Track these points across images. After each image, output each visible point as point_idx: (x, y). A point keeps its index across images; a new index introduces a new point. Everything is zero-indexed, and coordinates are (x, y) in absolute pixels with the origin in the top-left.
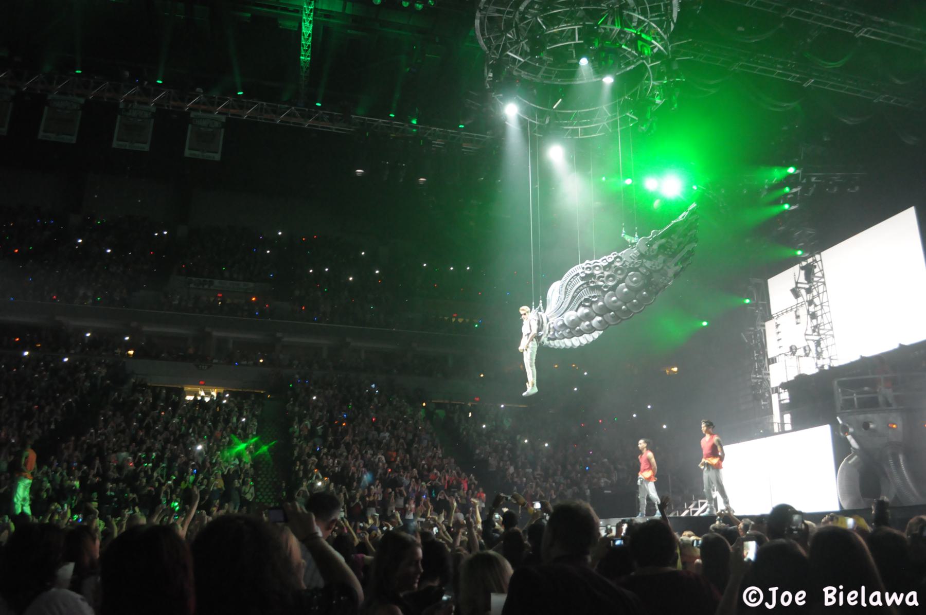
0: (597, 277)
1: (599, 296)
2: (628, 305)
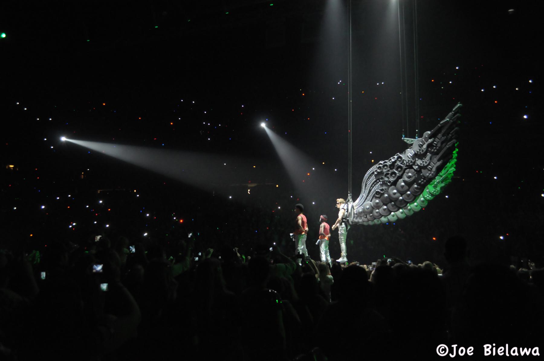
0: (384, 174)
1: (385, 189)
2: (403, 196)
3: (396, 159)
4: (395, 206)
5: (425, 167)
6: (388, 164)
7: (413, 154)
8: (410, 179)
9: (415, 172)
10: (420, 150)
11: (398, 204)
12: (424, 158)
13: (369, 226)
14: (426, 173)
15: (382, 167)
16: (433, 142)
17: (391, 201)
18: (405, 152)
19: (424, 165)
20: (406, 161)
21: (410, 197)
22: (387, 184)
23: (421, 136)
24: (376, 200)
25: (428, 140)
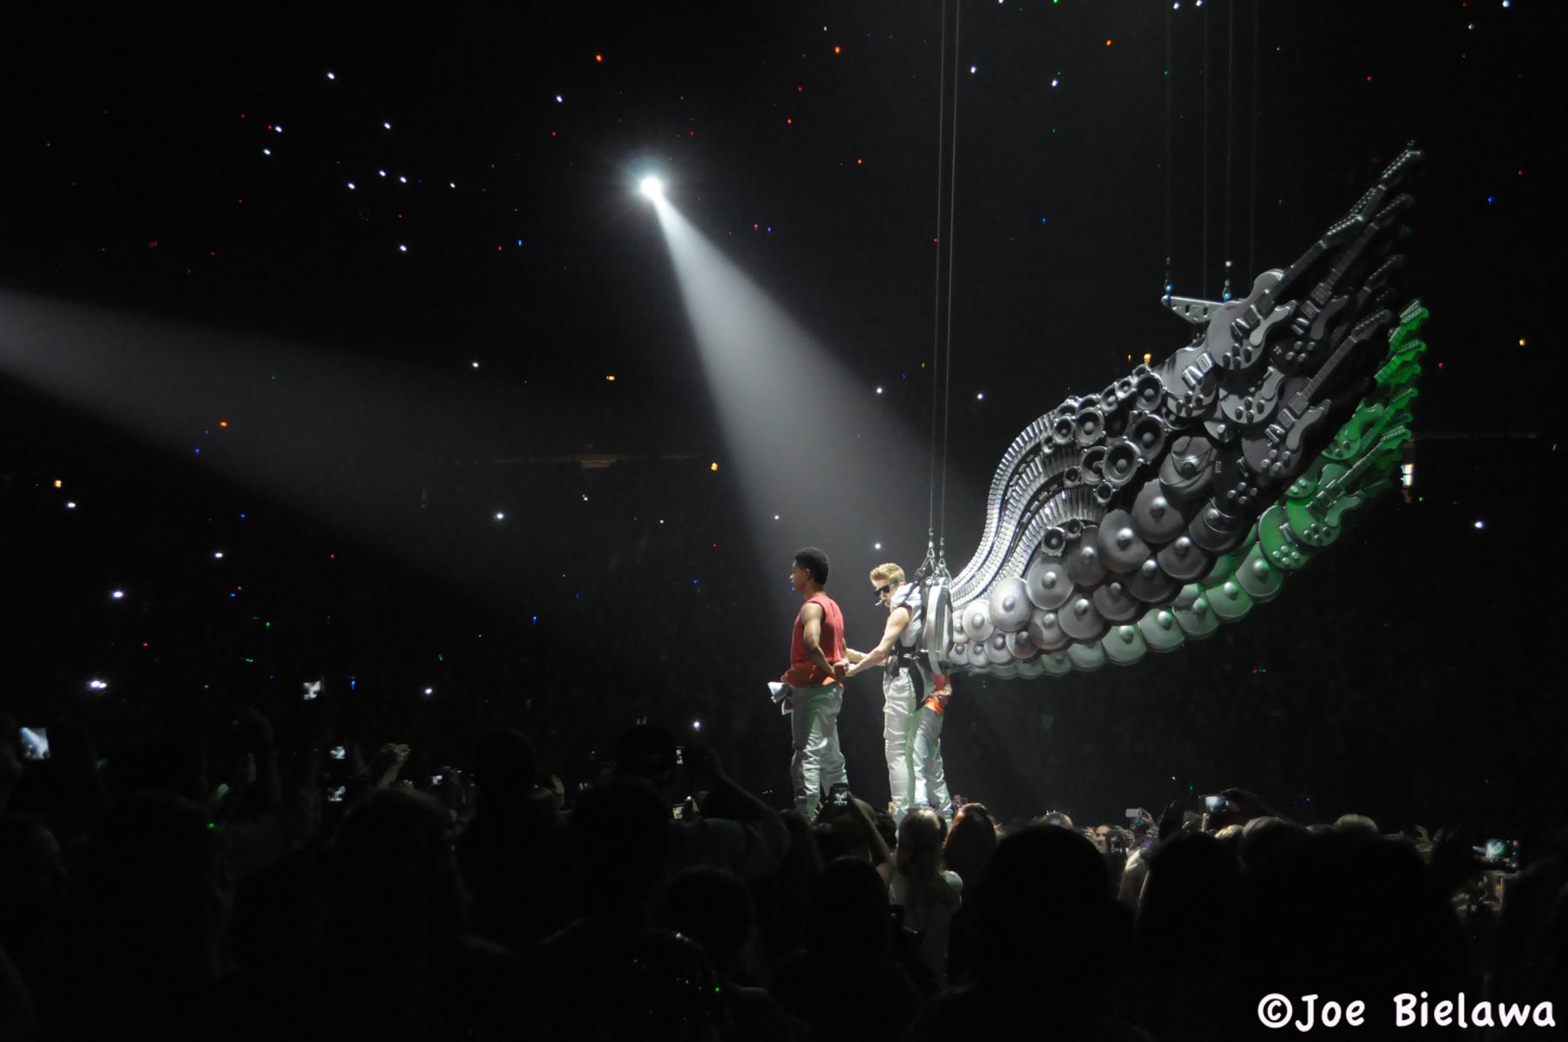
0: (1084, 456)
1: (1086, 522)
2: (1160, 555)
3: (1134, 390)
4: (1124, 602)
5: (1256, 431)
6: (1100, 412)
7: (1205, 371)
8: (1196, 478)
9: (1215, 451)
10: (1238, 355)
11: (1136, 590)
12: (1252, 389)
13: (1019, 682)
14: (1261, 457)
15: (1074, 424)
16: (1291, 319)
17: (1108, 579)
18: (1173, 362)
19: (1251, 418)
20: (1176, 399)
21: (1189, 559)
22: (1095, 499)
23: (1241, 291)
24: (1047, 572)
25: (1272, 310)
